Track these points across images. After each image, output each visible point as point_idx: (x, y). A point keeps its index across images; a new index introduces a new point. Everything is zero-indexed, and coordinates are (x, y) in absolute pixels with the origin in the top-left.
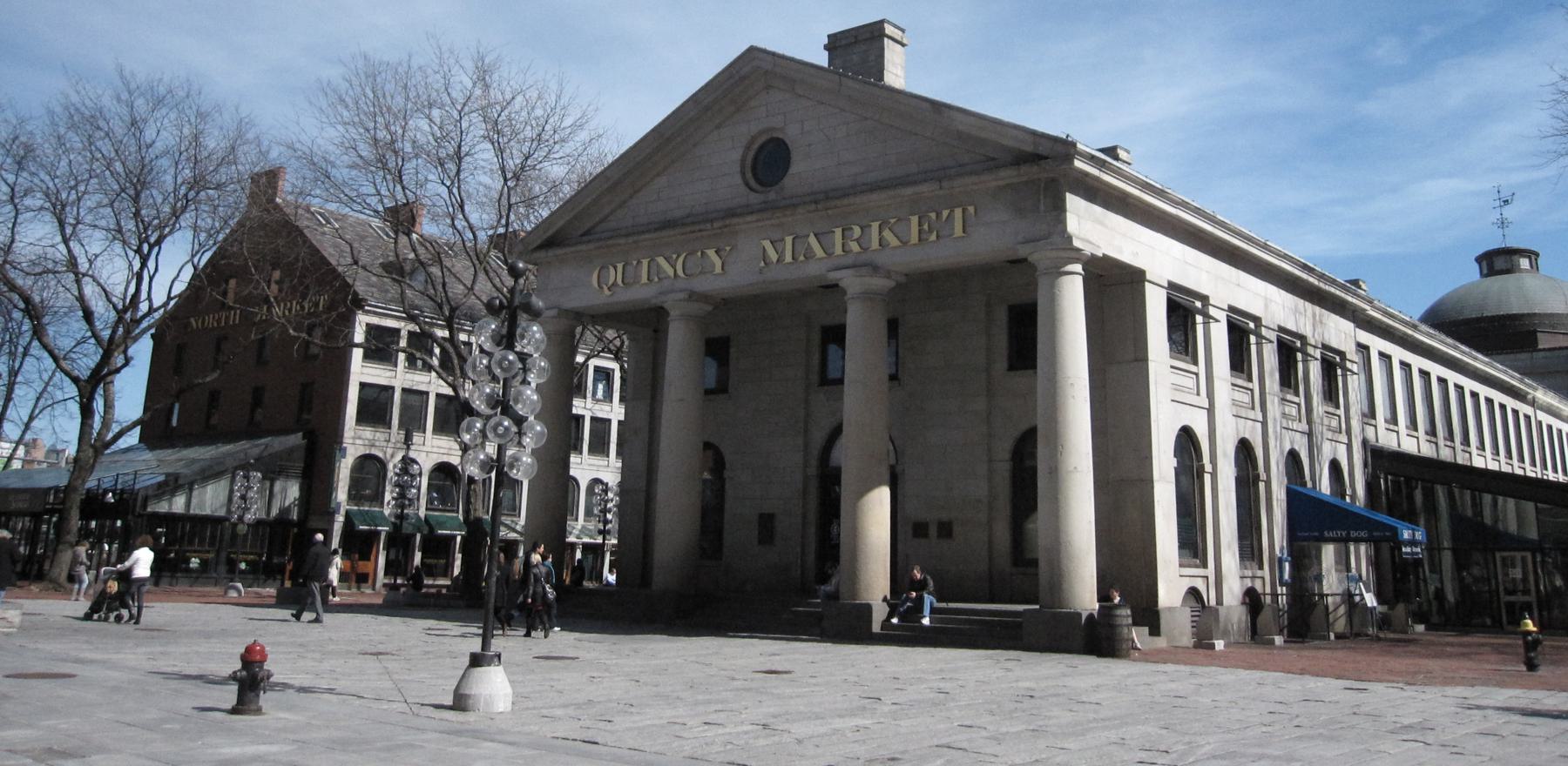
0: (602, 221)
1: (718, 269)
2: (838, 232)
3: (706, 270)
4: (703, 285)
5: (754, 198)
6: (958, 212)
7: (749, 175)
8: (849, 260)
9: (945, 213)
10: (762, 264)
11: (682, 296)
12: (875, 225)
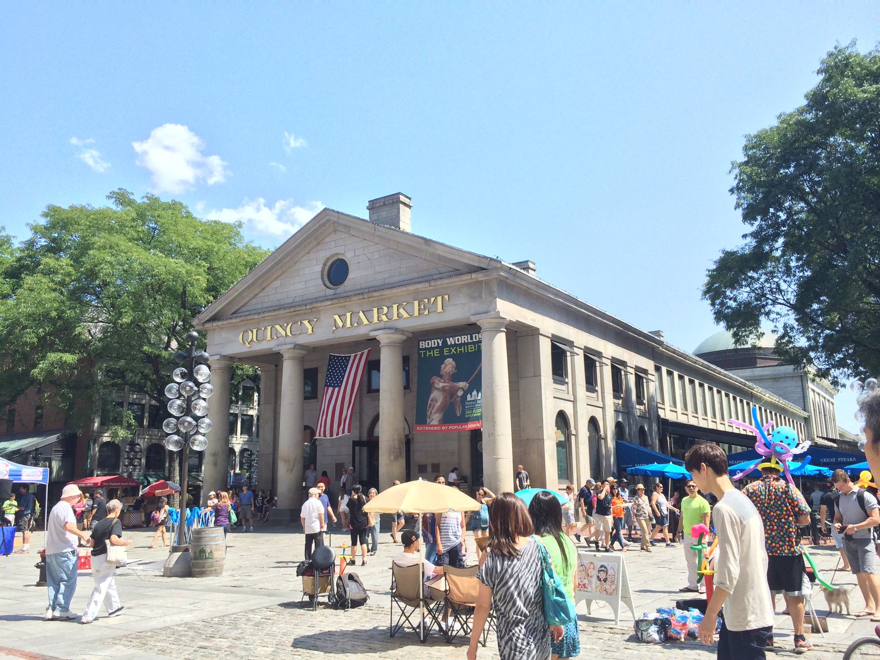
0: (244, 306)
1: (310, 331)
2: (375, 310)
3: (304, 332)
4: (302, 340)
5: (330, 292)
6: (440, 298)
7: (326, 279)
8: (382, 325)
9: (433, 299)
10: (334, 328)
11: (292, 346)
12: (395, 306)
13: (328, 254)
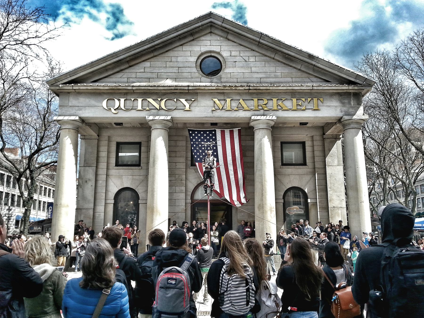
1: (187, 108)
4: (178, 114)
9: (309, 99)
13: (204, 49)
